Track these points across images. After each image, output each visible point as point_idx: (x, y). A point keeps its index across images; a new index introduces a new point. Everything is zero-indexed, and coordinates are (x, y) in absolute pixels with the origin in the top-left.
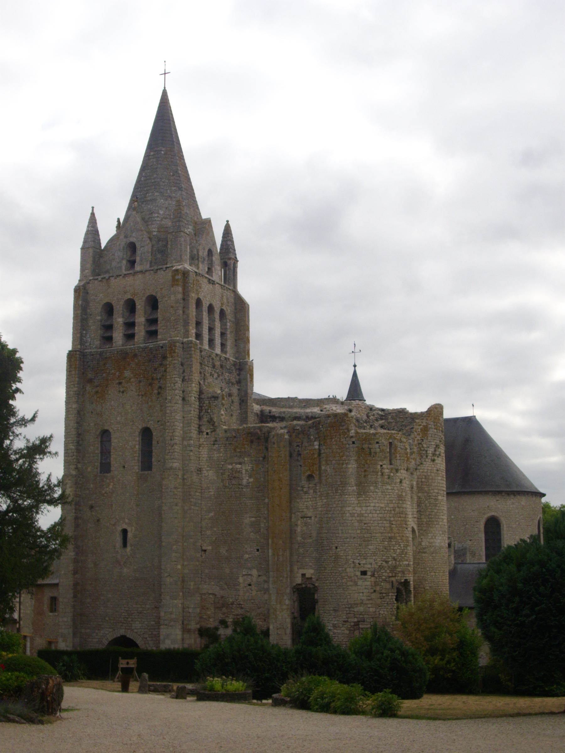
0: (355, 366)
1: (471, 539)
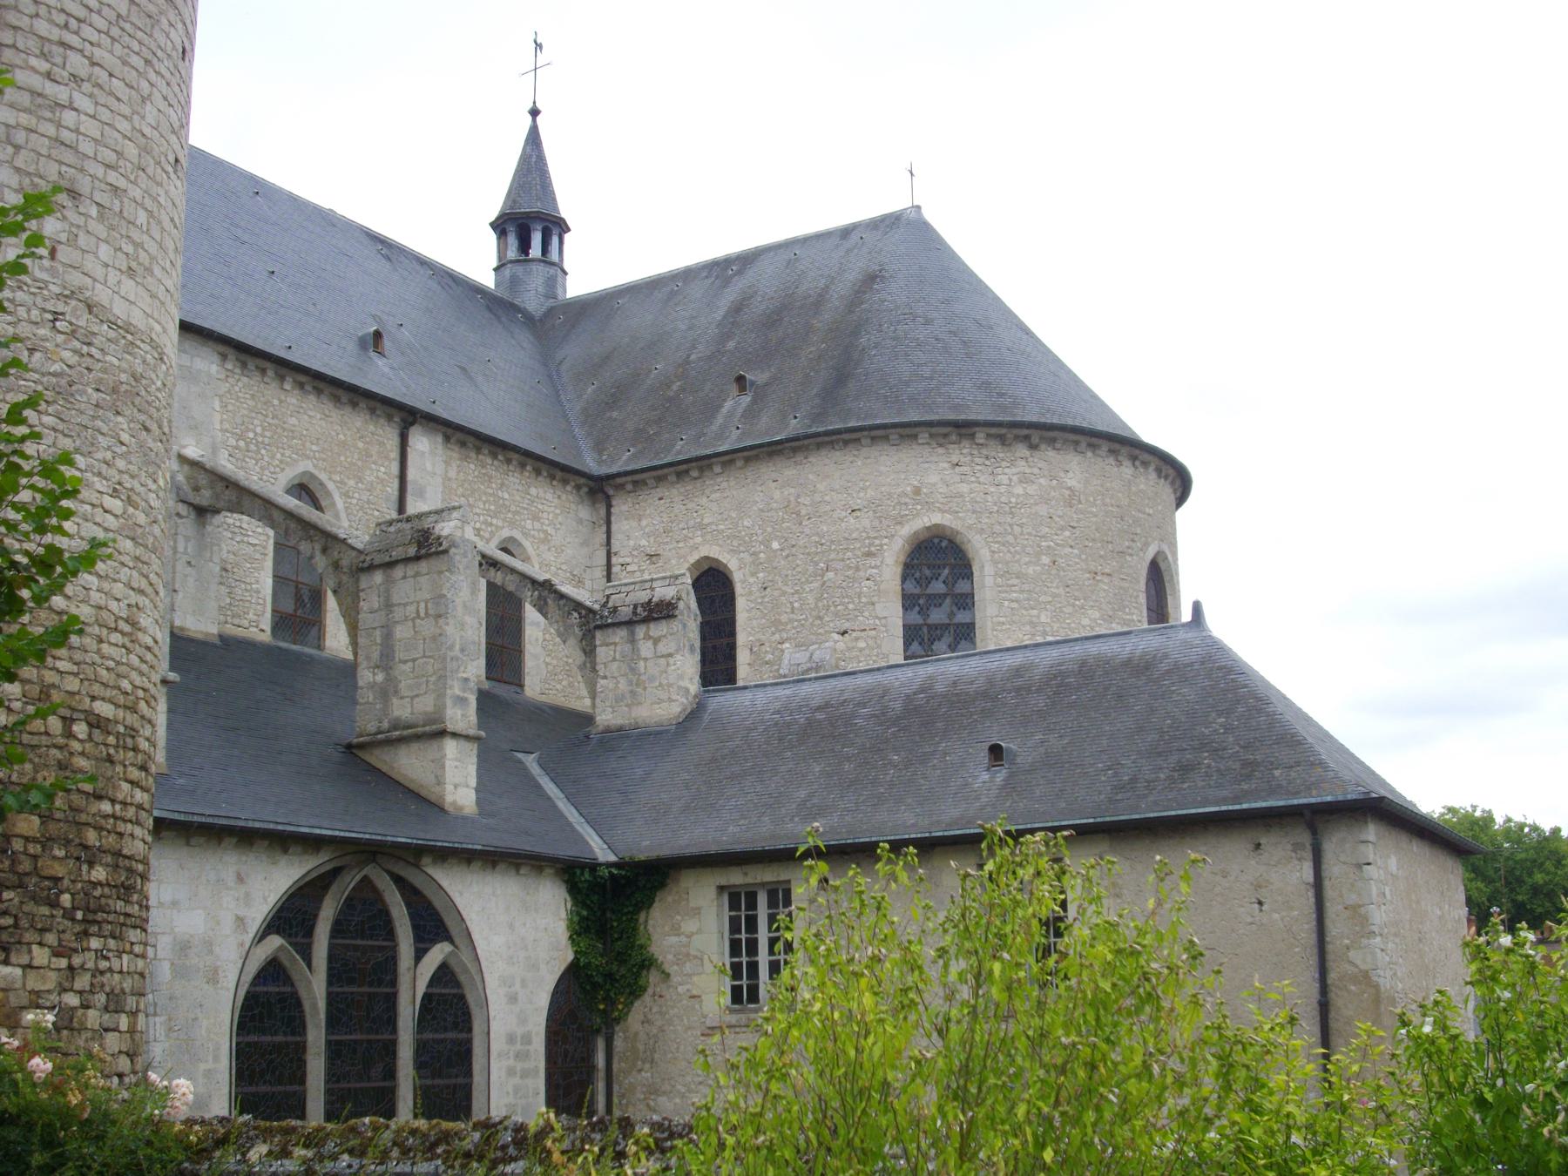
0: (535, 112)
1: (847, 625)
